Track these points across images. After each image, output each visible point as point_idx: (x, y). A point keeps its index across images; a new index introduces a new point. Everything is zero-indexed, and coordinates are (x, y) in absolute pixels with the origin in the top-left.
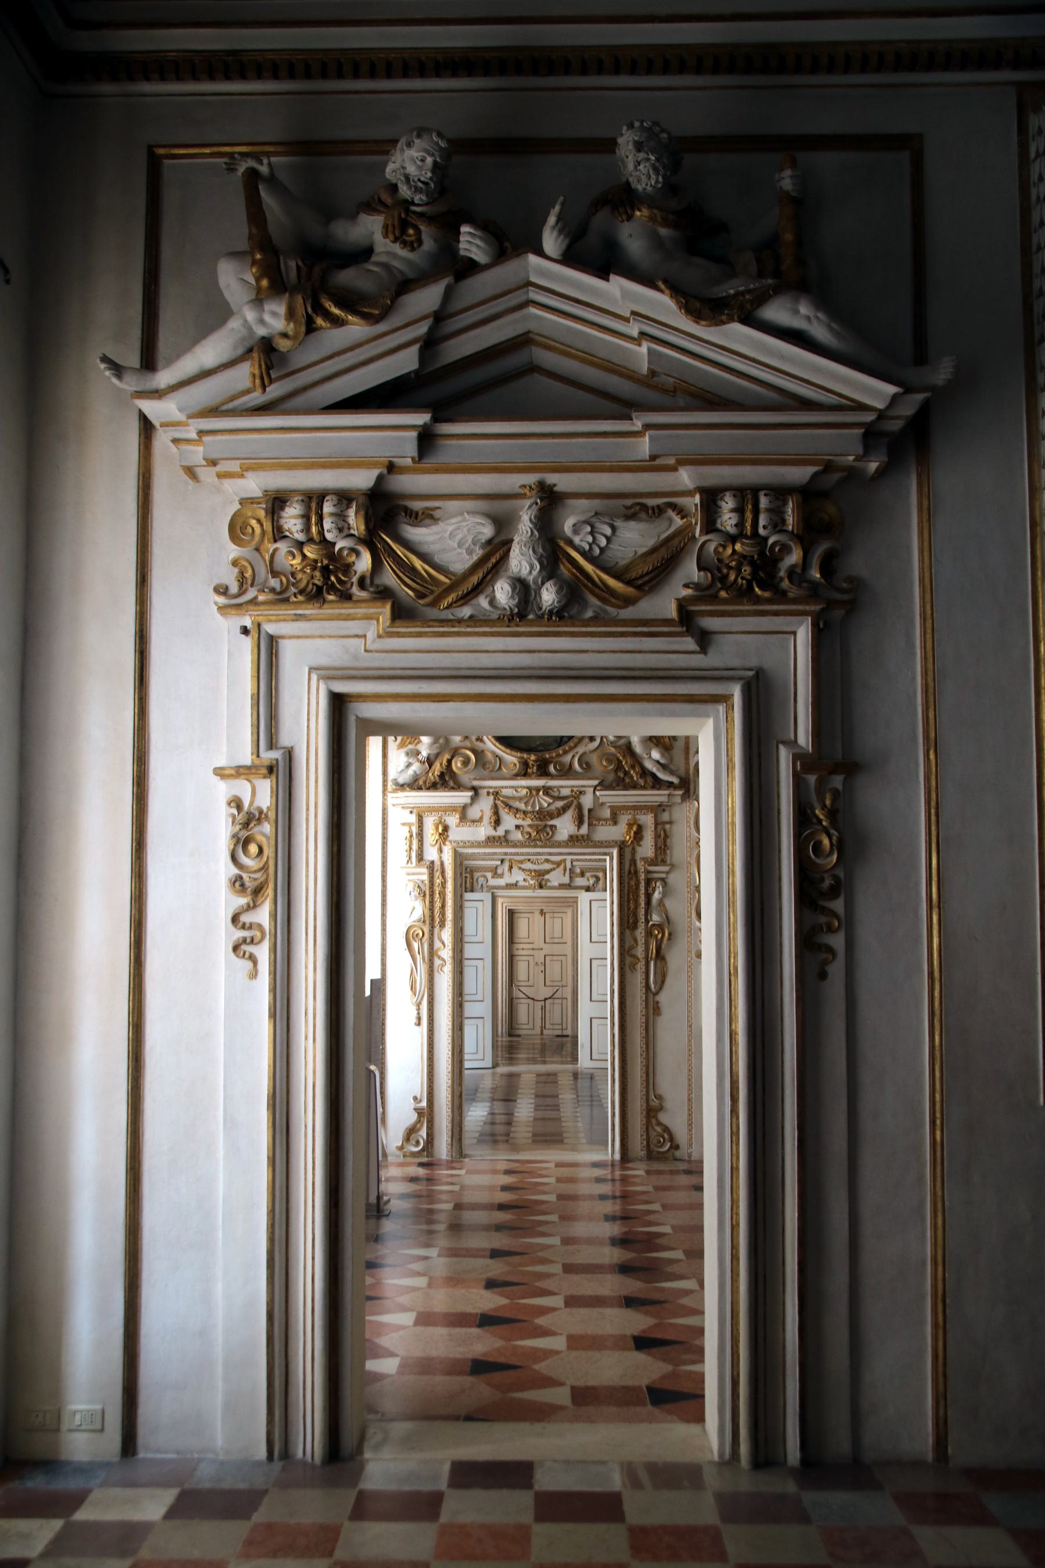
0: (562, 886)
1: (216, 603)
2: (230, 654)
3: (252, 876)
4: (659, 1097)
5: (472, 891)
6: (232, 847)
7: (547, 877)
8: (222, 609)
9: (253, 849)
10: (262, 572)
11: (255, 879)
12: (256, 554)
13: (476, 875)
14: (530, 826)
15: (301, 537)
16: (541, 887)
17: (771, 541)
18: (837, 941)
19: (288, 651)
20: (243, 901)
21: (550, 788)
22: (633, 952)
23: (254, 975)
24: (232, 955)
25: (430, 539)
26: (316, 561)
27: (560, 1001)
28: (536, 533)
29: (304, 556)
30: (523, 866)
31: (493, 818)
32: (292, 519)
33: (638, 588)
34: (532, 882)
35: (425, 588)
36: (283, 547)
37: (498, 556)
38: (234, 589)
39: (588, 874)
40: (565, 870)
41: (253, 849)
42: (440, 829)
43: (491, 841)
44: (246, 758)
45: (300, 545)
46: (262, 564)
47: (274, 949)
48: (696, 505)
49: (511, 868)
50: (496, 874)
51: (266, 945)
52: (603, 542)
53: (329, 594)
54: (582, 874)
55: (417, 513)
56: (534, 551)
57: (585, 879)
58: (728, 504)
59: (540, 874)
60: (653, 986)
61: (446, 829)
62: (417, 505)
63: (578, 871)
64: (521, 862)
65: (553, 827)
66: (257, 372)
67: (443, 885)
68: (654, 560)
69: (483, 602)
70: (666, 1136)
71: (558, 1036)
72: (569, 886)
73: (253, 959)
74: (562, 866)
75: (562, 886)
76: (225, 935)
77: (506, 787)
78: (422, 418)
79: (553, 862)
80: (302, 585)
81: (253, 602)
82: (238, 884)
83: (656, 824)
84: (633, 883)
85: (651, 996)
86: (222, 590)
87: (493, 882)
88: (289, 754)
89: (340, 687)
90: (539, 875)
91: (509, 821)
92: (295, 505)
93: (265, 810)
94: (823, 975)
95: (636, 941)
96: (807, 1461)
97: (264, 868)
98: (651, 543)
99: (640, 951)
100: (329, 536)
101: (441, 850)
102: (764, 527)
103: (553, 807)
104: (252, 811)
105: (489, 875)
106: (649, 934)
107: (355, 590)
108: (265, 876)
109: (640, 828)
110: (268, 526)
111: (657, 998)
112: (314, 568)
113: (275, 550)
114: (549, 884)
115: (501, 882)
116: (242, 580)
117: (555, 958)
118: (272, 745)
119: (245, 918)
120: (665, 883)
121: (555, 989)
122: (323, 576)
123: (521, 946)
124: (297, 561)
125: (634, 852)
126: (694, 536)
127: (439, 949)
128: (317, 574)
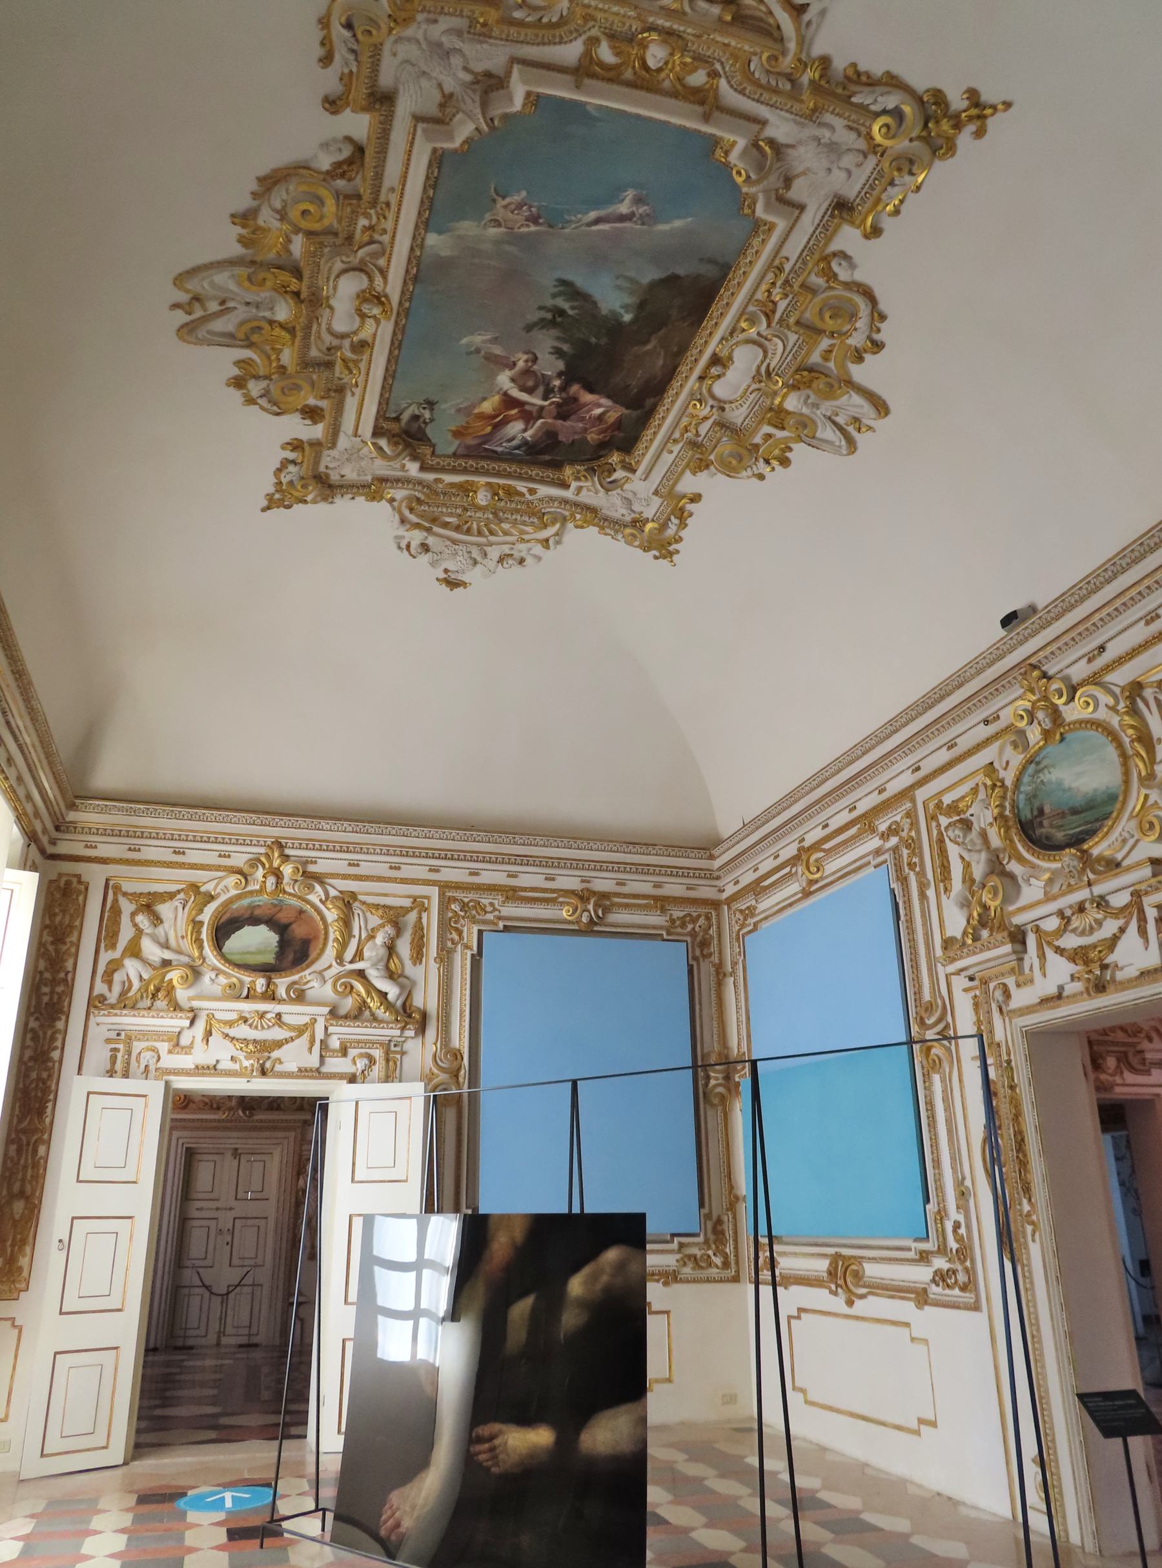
0: (303, 1073)
5: (126, 1075)
7: (275, 1054)
13: (137, 1046)
16: (263, 1073)
27: (248, 1290)
30: (232, 1032)
34: (247, 1063)
39: (352, 1052)
49: (208, 1033)
50: (176, 1044)
54: (344, 1051)
59: (266, 1047)
63: (335, 1043)
64: (230, 1024)
71: (241, 1346)
72: (317, 1073)
74: (306, 1036)
75: (303, 1073)
79: (291, 1028)
90: (261, 1051)
105: (163, 1047)
114: (278, 1068)
115: (186, 1061)
117: (250, 1222)
121: (246, 1269)
123: (199, 1204)
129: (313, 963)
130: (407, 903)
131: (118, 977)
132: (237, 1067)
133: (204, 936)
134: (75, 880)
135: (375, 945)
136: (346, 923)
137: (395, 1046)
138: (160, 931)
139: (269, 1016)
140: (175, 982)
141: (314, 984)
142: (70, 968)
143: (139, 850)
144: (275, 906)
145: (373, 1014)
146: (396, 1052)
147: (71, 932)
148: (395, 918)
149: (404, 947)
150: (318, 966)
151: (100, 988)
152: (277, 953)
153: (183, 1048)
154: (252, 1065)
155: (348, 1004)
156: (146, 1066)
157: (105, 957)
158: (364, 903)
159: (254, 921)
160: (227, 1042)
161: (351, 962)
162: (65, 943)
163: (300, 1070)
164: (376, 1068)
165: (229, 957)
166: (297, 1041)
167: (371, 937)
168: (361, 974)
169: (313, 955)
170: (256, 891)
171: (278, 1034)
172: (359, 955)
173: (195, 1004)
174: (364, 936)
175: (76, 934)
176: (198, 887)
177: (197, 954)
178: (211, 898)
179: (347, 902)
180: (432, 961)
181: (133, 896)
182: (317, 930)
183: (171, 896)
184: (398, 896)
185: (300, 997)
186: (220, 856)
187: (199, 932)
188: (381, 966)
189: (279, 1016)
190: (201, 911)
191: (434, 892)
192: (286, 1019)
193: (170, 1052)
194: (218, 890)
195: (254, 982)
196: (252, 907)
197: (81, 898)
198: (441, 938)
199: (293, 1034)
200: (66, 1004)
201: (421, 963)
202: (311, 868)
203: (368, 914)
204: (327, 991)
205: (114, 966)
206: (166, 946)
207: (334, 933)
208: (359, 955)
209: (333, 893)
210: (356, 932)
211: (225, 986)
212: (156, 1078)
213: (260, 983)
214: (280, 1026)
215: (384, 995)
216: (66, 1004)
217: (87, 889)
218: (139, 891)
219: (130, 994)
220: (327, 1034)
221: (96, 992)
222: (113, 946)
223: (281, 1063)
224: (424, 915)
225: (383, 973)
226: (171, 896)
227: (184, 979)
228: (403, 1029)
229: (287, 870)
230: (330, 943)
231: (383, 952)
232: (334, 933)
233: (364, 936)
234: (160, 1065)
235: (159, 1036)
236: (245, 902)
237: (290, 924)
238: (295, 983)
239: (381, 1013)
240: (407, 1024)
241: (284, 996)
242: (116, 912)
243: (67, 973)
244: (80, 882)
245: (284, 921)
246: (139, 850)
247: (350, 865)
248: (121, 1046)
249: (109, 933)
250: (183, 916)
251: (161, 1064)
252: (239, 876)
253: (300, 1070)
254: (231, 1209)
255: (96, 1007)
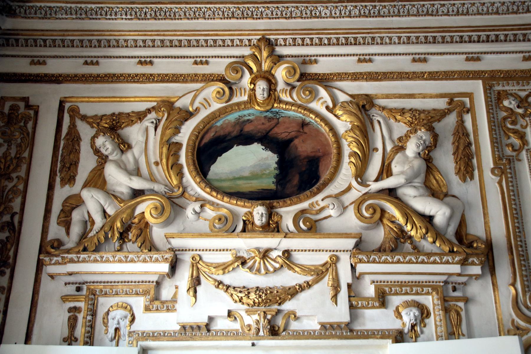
7: (288, 306)
30: (227, 279)
39: (396, 300)
40: (336, 288)
49: (196, 282)
50: (156, 301)
54: (382, 299)
57: (390, 312)
63: (370, 291)
64: (224, 268)
74: (327, 280)
79: (305, 269)
87: (147, 322)
90: (267, 302)
105: (138, 303)
114: (294, 325)
129: (326, 184)
130: (441, 104)
131: (77, 216)
132: (236, 326)
133: (183, 160)
134: (22, 105)
135: (407, 157)
136: (364, 131)
137: (454, 289)
138: (129, 157)
139: (274, 254)
140: (147, 216)
141: (331, 212)
142: (17, 209)
143: (97, 63)
144: (270, 119)
145: (415, 248)
146: (458, 299)
147: (18, 166)
148: (427, 120)
149: (446, 160)
150: (333, 189)
151: (55, 231)
152: (277, 176)
153: (163, 303)
154: (258, 322)
155: (379, 236)
156: (117, 330)
157: (61, 193)
158: (384, 108)
159: (246, 139)
160: (221, 292)
161: (377, 180)
162: (10, 179)
163: (323, 326)
164: (431, 321)
165: (217, 184)
166: (316, 287)
167: (400, 148)
168: (391, 193)
169: (325, 176)
170: (244, 103)
171: (289, 278)
172: (386, 171)
173: (176, 243)
174: (389, 147)
175: (24, 167)
176: (173, 103)
177: (175, 182)
178: (188, 115)
179: (363, 106)
180: (488, 175)
181: (94, 121)
182: (326, 145)
183: (141, 116)
184: (428, 96)
185: (312, 227)
186: (196, 63)
187: (177, 156)
188: (418, 182)
189: (287, 254)
190: (177, 131)
191: (477, 87)
192: (300, 258)
193: (147, 309)
194: (196, 104)
195: (251, 213)
196: (241, 123)
197: (30, 125)
198: (495, 142)
199: (309, 278)
200: (11, 253)
201: (472, 178)
202: (314, 69)
203: (392, 121)
204: (351, 221)
205: (74, 203)
206: (137, 172)
207: (349, 147)
208: (386, 171)
209: (342, 97)
210: (379, 145)
211: (214, 218)
212: (130, 344)
213: (259, 213)
214: (290, 268)
215: (429, 219)
216: (11, 253)
217: (36, 113)
218: (100, 113)
219: (91, 235)
220: (357, 277)
221: (51, 236)
222: (70, 180)
223: (296, 318)
224: (468, 119)
225: (422, 191)
226: (141, 116)
227: (160, 211)
228: (464, 263)
229: (281, 73)
230: (346, 159)
231: (418, 163)
232: (349, 147)
233: (389, 147)
234: (135, 327)
235: (133, 288)
236: (232, 117)
237: (291, 140)
238: (303, 211)
239: (427, 245)
240: (468, 256)
241: (292, 228)
242: (74, 139)
243: (13, 215)
244: (28, 106)
245: (284, 136)
246: (97, 63)
247: (360, 61)
248: (81, 305)
249: (65, 165)
250: (154, 140)
251: (135, 327)
252: (221, 85)
253: (323, 326)
255: (49, 254)
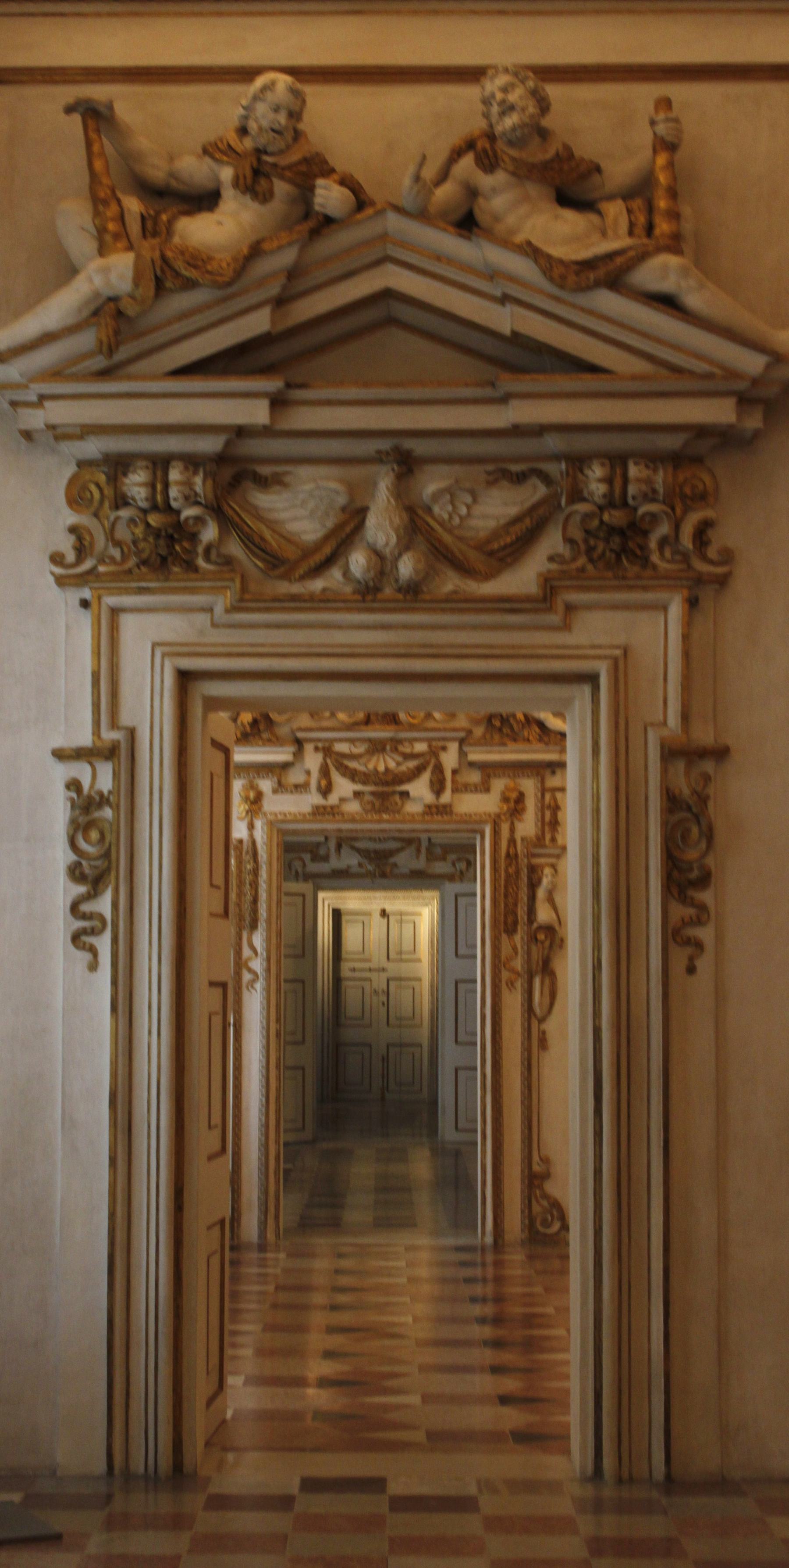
1: (52, 573)
2: (68, 627)
3: (92, 863)
4: (546, 1161)
6: (71, 832)
7: (392, 860)
8: (60, 581)
9: (94, 835)
10: (100, 541)
11: (96, 867)
12: (95, 520)
14: (373, 793)
15: (144, 504)
17: (642, 510)
18: (706, 934)
19: (129, 624)
20: (82, 889)
21: (401, 741)
22: (513, 964)
23: (93, 966)
24: (72, 948)
25: (279, 505)
26: (159, 530)
28: (392, 500)
29: (148, 525)
31: (324, 783)
32: (136, 485)
33: (501, 560)
34: (370, 868)
35: (275, 563)
36: (125, 513)
37: (352, 525)
38: (71, 557)
41: (94, 835)
42: (252, 795)
43: (319, 812)
44: (85, 739)
45: (145, 512)
46: (101, 530)
47: (115, 940)
48: (561, 473)
51: (107, 936)
52: (463, 511)
53: (175, 565)
55: (266, 479)
56: (391, 522)
58: (597, 471)
60: (538, 1010)
61: (259, 796)
62: (265, 470)
65: (405, 795)
66: (105, 339)
67: (256, 872)
68: (518, 529)
69: (336, 573)
70: (555, 1213)
73: (93, 951)
76: (61, 925)
77: (341, 740)
78: (273, 384)
80: (144, 556)
81: (91, 572)
82: (75, 873)
83: (543, 791)
84: (511, 870)
85: (535, 1023)
86: (57, 559)
88: (132, 733)
89: (187, 664)
91: (344, 787)
92: (142, 473)
93: (106, 793)
94: (691, 970)
95: (515, 949)
96: (668, 1477)
97: (107, 855)
98: (513, 511)
99: (518, 964)
100: (174, 504)
101: (251, 827)
102: (634, 498)
103: (403, 768)
104: (93, 793)
105: (307, 857)
106: (533, 938)
107: (201, 562)
108: (106, 863)
109: (521, 798)
110: (108, 491)
111: (544, 1026)
112: (158, 536)
113: (117, 519)
115: (325, 867)
116: (81, 551)
118: (114, 725)
119: (85, 908)
120: (556, 871)
122: (168, 546)
124: (139, 531)
125: (512, 830)
126: (559, 505)
127: (249, 959)
128: (162, 542)
132: (363, 871)
254: (384, 970)
